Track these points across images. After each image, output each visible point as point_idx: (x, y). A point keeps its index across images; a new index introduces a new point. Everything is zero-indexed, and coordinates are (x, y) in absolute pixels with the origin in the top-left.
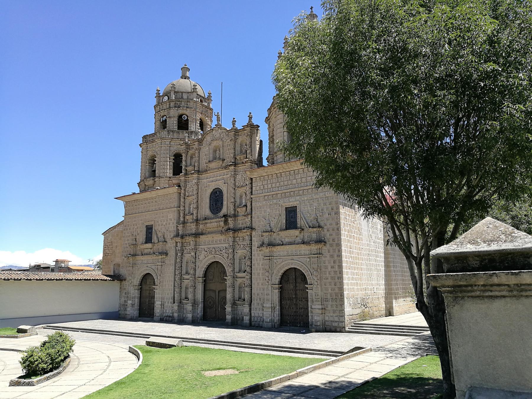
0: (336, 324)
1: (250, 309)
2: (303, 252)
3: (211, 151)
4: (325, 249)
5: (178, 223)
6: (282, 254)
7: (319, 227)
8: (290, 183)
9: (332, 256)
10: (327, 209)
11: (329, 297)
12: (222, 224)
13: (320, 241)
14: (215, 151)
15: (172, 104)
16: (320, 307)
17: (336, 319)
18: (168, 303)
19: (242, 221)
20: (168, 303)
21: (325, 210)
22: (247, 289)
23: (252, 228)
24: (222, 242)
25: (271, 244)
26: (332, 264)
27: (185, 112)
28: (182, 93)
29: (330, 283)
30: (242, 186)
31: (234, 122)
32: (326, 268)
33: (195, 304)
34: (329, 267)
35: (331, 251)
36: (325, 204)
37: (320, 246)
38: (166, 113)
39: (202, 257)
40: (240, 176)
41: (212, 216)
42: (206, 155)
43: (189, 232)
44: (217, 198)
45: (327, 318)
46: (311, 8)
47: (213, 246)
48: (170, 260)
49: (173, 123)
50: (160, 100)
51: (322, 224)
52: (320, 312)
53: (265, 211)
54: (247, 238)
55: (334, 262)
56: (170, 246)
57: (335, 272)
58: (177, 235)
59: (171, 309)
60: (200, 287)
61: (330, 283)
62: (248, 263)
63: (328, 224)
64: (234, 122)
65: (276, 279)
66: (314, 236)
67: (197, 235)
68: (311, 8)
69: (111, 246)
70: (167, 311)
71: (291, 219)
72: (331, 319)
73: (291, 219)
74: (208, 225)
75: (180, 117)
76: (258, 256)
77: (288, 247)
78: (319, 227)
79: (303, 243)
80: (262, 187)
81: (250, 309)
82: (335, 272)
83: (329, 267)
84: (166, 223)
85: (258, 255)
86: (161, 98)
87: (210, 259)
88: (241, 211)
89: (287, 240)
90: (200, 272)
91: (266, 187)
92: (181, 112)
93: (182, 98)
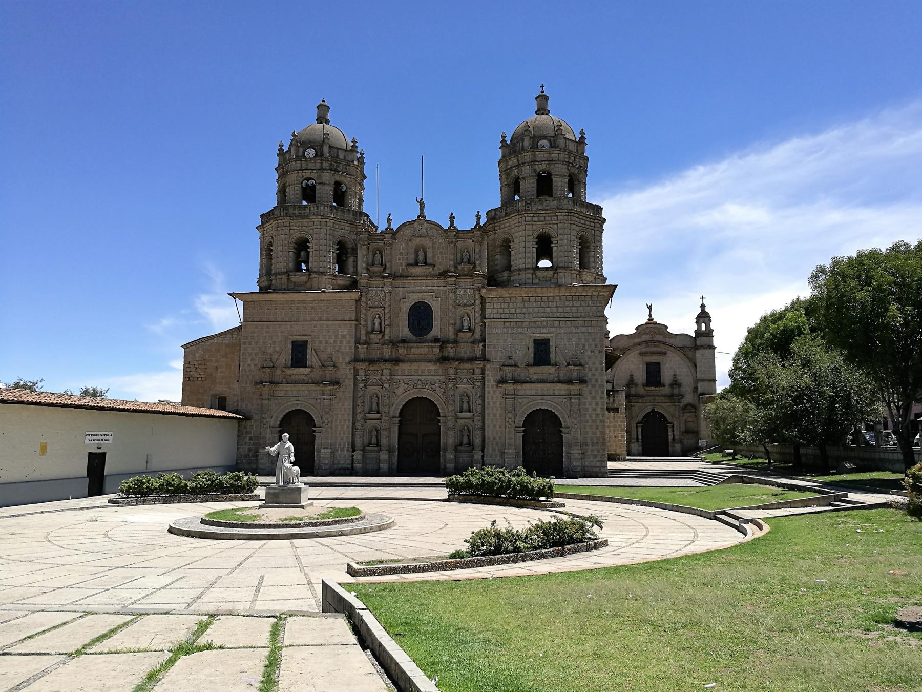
0: (598, 470)
1: (483, 456)
2: (557, 392)
3: (412, 251)
4: (586, 389)
5: (357, 341)
6: (528, 392)
7: (580, 365)
8: (541, 310)
9: (594, 398)
10: (590, 345)
11: (588, 441)
12: (437, 350)
13: (582, 381)
14: (416, 252)
15: (325, 165)
16: (580, 452)
17: (598, 464)
18: (342, 450)
19: (465, 350)
20: (342, 450)
21: (587, 347)
22: (479, 432)
23: (484, 358)
24: (433, 373)
25: (516, 381)
26: (594, 406)
27: (343, 179)
28: (338, 149)
29: (591, 427)
30: (465, 305)
31: (452, 218)
32: (587, 409)
33: (390, 450)
34: (590, 411)
35: (593, 392)
36: (587, 340)
37: (581, 386)
38: (314, 175)
39: (399, 391)
40: (462, 291)
41: (414, 338)
42: (401, 254)
43: (375, 354)
44: (421, 317)
45: (587, 464)
46: (542, 86)
47: (420, 377)
48: (346, 393)
49: (325, 192)
50: (298, 151)
51: (583, 363)
52: (579, 457)
53: (505, 340)
54: (478, 371)
55: (597, 404)
56: (345, 372)
57: (597, 415)
58: (356, 360)
59: (343, 456)
60: (396, 429)
61: (591, 427)
62: (480, 402)
63: (590, 363)
64: (452, 218)
65: (520, 421)
66: (575, 375)
67: (397, 361)
68: (542, 86)
69: (204, 367)
70: (342, 462)
71: (542, 352)
72: (592, 464)
73: (542, 352)
74: (413, 350)
75: (338, 184)
76: (494, 396)
77: (540, 385)
78: (580, 365)
79: (559, 382)
80: (501, 311)
81: (483, 456)
82: (597, 415)
83: (590, 411)
84: (334, 339)
85: (494, 392)
86: (301, 150)
87: (413, 394)
88: (465, 336)
89: (535, 377)
90: (396, 410)
91: (507, 311)
92: (338, 178)
93: (337, 156)
